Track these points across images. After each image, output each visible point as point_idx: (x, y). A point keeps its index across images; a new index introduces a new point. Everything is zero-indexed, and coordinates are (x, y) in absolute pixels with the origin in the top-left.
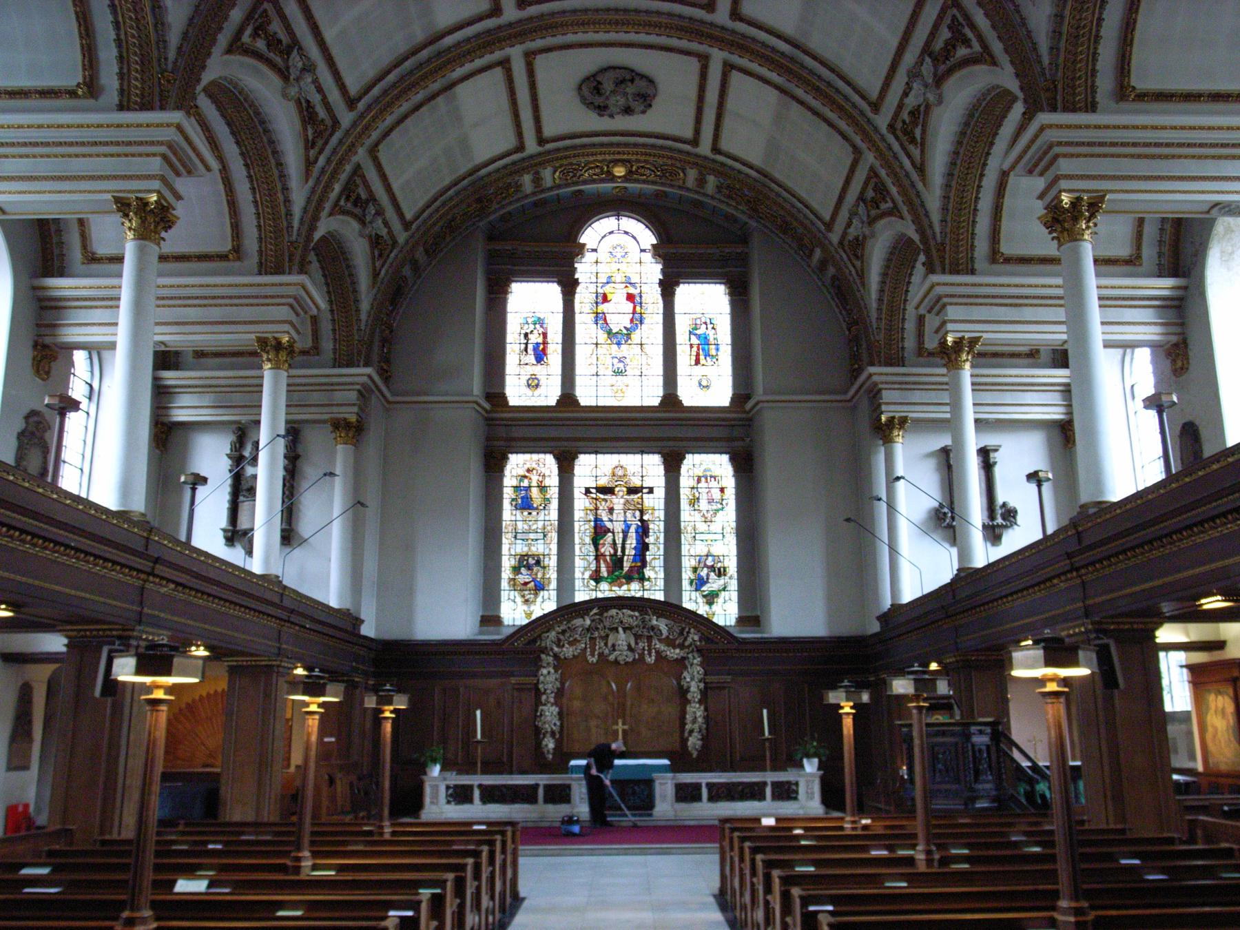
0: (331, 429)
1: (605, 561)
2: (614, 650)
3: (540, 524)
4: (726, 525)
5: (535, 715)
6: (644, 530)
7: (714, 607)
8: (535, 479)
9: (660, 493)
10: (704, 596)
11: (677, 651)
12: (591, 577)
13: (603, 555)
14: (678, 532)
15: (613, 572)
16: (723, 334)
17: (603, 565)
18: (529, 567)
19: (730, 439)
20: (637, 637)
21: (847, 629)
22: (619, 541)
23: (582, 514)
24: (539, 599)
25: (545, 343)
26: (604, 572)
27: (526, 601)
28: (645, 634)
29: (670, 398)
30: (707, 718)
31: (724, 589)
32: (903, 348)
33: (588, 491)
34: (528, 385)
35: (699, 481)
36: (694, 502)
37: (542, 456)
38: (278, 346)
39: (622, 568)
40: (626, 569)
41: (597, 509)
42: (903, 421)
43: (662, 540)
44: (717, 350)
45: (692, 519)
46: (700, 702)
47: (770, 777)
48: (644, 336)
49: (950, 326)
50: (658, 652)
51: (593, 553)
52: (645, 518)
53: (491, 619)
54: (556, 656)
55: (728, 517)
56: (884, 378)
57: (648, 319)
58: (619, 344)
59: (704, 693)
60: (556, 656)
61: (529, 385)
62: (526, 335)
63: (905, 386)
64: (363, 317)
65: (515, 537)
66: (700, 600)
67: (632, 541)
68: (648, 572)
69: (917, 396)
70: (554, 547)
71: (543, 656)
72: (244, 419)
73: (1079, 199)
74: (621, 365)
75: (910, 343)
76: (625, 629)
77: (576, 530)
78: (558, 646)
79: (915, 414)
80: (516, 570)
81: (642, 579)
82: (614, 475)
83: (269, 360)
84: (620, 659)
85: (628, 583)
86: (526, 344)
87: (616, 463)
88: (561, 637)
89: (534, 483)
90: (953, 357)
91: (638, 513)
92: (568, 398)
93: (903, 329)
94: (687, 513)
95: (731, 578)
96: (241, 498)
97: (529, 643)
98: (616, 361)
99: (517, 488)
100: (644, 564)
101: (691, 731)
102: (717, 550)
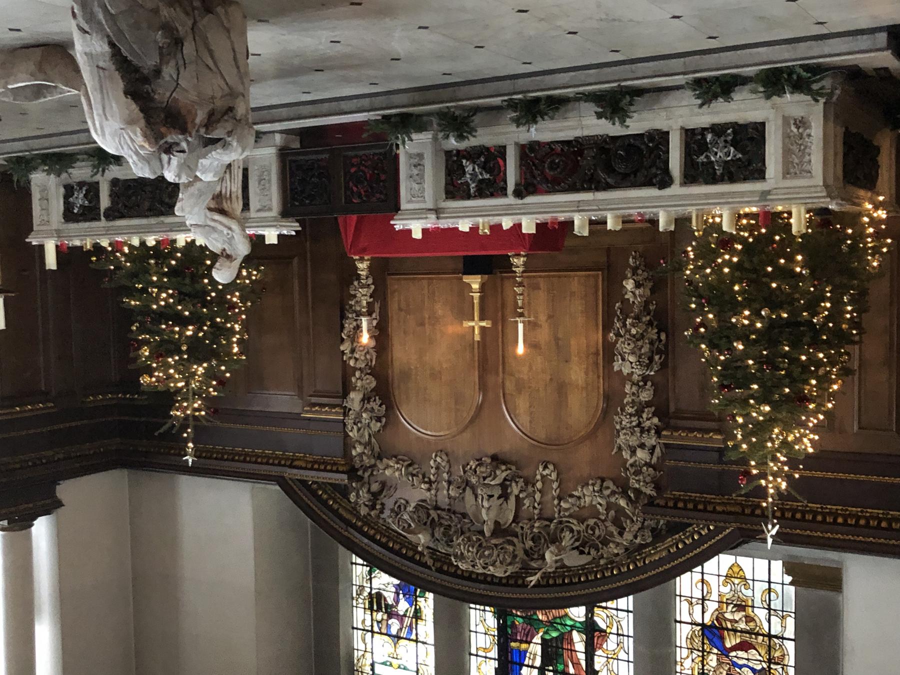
1: (576, 664)
2: (504, 486)
17: (582, 657)
21: (154, 482)
24: (712, 606)
26: (579, 642)
39: (545, 643)
40: (537, 639)
60: (623, 488)
71: (649, 491)
78: (620, 510)
88: (613, 529)
97: (682, 527)
102: (381, 647)
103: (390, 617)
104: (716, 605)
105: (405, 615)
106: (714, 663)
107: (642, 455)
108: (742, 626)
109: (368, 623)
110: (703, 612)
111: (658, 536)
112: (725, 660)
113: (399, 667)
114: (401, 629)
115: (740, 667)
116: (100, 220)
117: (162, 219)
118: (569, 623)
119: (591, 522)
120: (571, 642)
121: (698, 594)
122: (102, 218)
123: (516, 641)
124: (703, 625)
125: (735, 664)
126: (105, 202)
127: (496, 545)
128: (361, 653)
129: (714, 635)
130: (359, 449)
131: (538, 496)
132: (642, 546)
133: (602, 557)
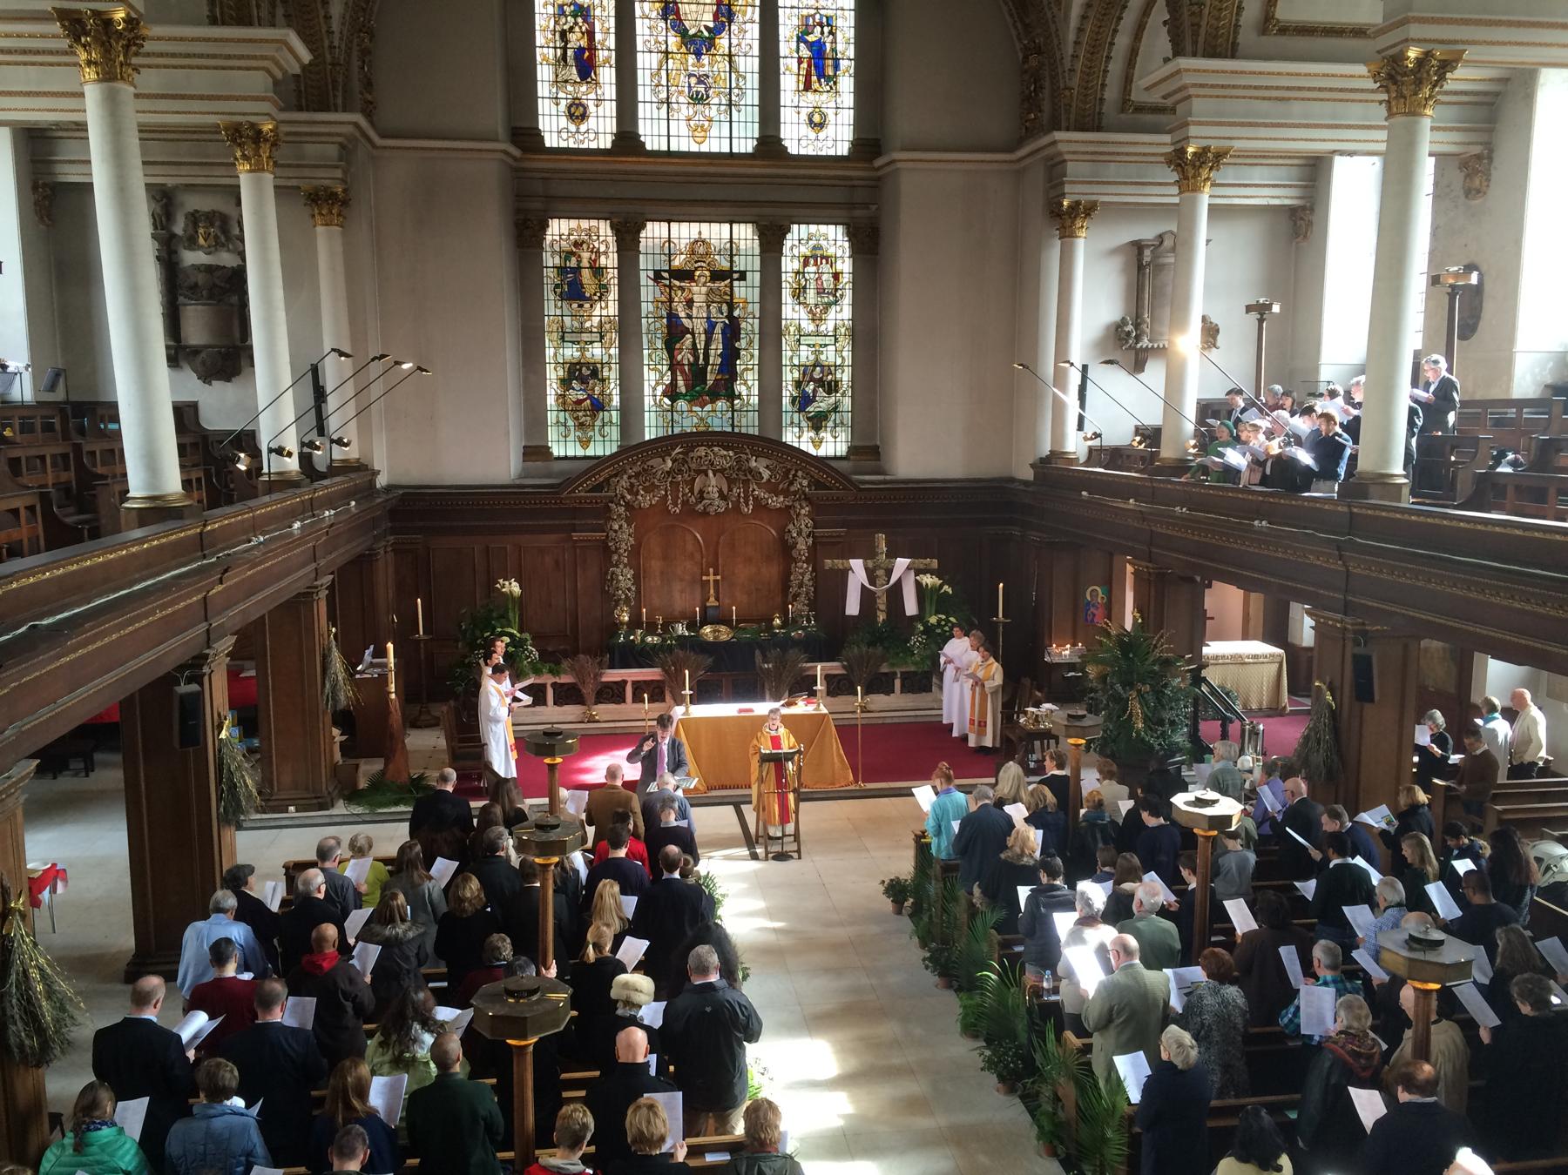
0: (303, 201)
1: (683, 372)
2: (702, 498)
3: (596, 321)
5: (605, 580)
6: (732, 331)
7: (822, 434)
8: (586, 255)
9: (755, 278)
12: (664, 394)
13: (681, 364)
14: (779, 334)
15: (693, 387)
16: (845, 42)
18: (583, 380)
19: (851, 205)
20: (731, 482)
22: (701, 346)
23: (651, 308)
24: (598, 423)
25: (592, 47)
28: (739, 476)
29: (769, 142)
30: (814, 579)
32: (1102, 100)
33: (658, 276)
34: (570, 121)
35: (806, 264)
36: (799, 292)
37: (594, 223)
38: (258, 136)
41: (671, 300)
42: (1089, 210)
44: (836, 67)
45: (796, 316)
46: (807, 561)
48: (734, 42)
49: (1193, 131)
50: (756, 499)
53: (536, 452)
54: (628, 506)
55: (843, 313)
56: (1073, 147)
57: (739, 18)
58: (698, 54)
59: (813, 549)
61: (571, 116)
62: (563, 34)
63: (1097, 158)
64: (335, 26)
65: (563, 338)
66: (804, 424)
67: (717, 347)
68: (739, 388)
69: (1112, 171)
70: (614, 351)
72: (170, 182)
73: (1428, 55)
74: (701, 88)
75: (1111, 94)
78: (630, 491)
79: (1106, 196)
80: (565, 383)
81: (732, 396)
82: (693, 252)
83: (246, 158)
84: (711, 510)
85: (713, 402)
86: (565, 49)
87: (695, 236)
89: (585, 263)
90: (1191, 172)
92: (627, 138)
93: (1106, 71)
94: (789, 307)
95: (843, 395)
96: (181, 299)
98: (693, 80)
99: (562, 270)
101: (796, 596)
102: (829, 356)
107: (616, 527)
111: (607, 480)
121: (607, 429)
126: (898, 683)
132: (616, 475)
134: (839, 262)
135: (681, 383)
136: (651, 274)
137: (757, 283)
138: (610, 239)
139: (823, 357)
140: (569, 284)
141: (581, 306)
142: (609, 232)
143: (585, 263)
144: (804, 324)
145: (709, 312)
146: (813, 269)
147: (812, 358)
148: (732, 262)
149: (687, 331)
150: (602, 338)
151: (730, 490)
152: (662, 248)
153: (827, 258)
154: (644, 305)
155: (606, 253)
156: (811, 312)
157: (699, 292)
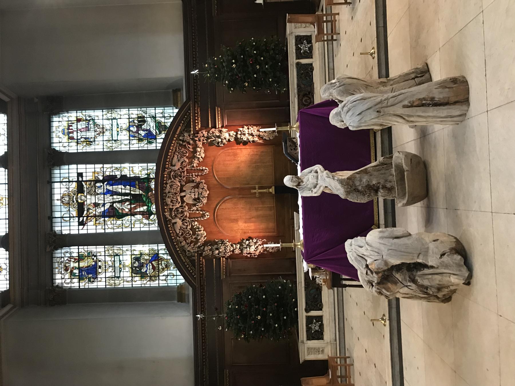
1: (135, 208)
3: (108, 259)
4: (105, 117)
6: (111, 180)
8: (72, 265)
9: (82, 168)
10: (160, 133)
11: (199, 149)
12: (148, 218)
13: (130, 210)
17: (138, 210)
18: (141, 266)
22: (120, 198)
23: (99, 227)
27: (167, 267)
31: (154, 117)
33: (81, 224)
35: (72, 138)
36: (89, 142)
39: (140, 195)
40: (141, 192)
41: (95, 216)
43: (118, 166)
45: (101, 143)
47: (292, 60)
50: (199, 164)
51: (129, 218)
52: (101, 178)
55: (97, 114)
67: (119, 188)
68: (143, 175)
70: (125, 248)
76: (182, 191)
77: (112, 231)
80: (143, 276)
81: (148, 179)
89: (76, 265)
91: (98, 185)
94: (97, 147)
99: (81, 278)
100: (137, 179)
102: (124, 123)
103: (137, 126)
104: (166, 258)
105: (139, 134)
106: (146, 258)
108: (160, 267)
109: (133, 116)
110: (163, 254)
111: (188, 257)
112: (148, 262)
113: (118, 132)
114: (133, 132)
115: (147, 267)
116: (296, 59)
117: (297, 96)
118: (150, 205)
119: (191, 233)
120: (143, 206)
122: (298, 61)
123: (139, 183)
124: (158, 254)
125: (147, 265)
126: (304, 61)
127: (177, 200)
128: (119, 112)
129: (156, 257)
130: (206, 135)
131: (198, 212)
132: (185, 252)
133: (180, 237)
134: (70, 119)
135: (142, 209)
136: (81, 227)
137: (83, 166)
138: (63, 251)
139: (125, 126)
140: (88, 274)
141: (100, 267)
142: (59, 251)
143: (76, 265)
144: (106, 138)
145: (101, 194)
146: (75, 133)
147: (125, 132)
148: (72, 182)
149: (111, 206)
150: (117, 255)
151: (193, 181)
152: (66, 221)
153: (69, 126)
154: (99, 231)
155: (70, 253)
156: (99, 134)
157: (90, 200)
